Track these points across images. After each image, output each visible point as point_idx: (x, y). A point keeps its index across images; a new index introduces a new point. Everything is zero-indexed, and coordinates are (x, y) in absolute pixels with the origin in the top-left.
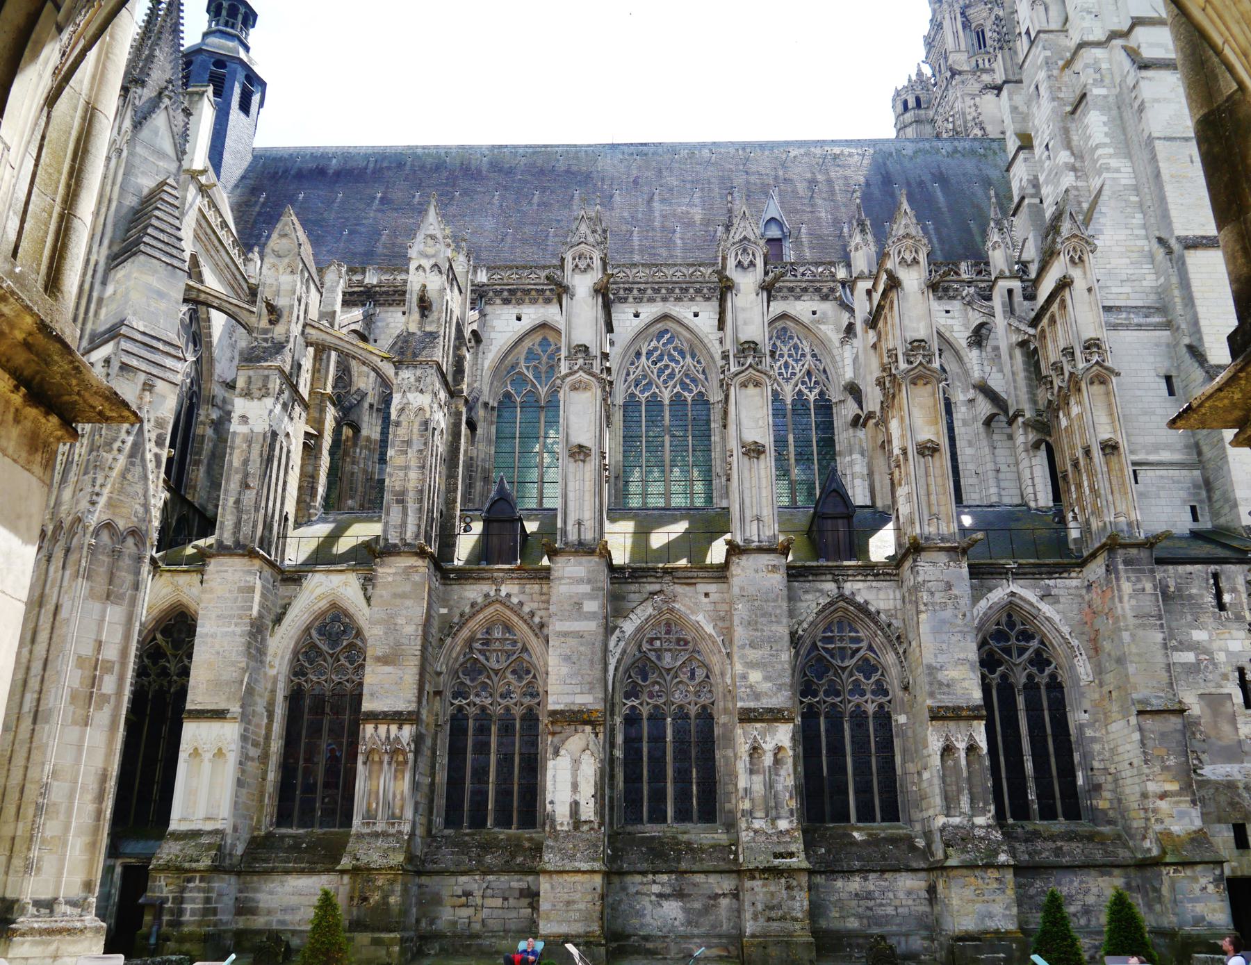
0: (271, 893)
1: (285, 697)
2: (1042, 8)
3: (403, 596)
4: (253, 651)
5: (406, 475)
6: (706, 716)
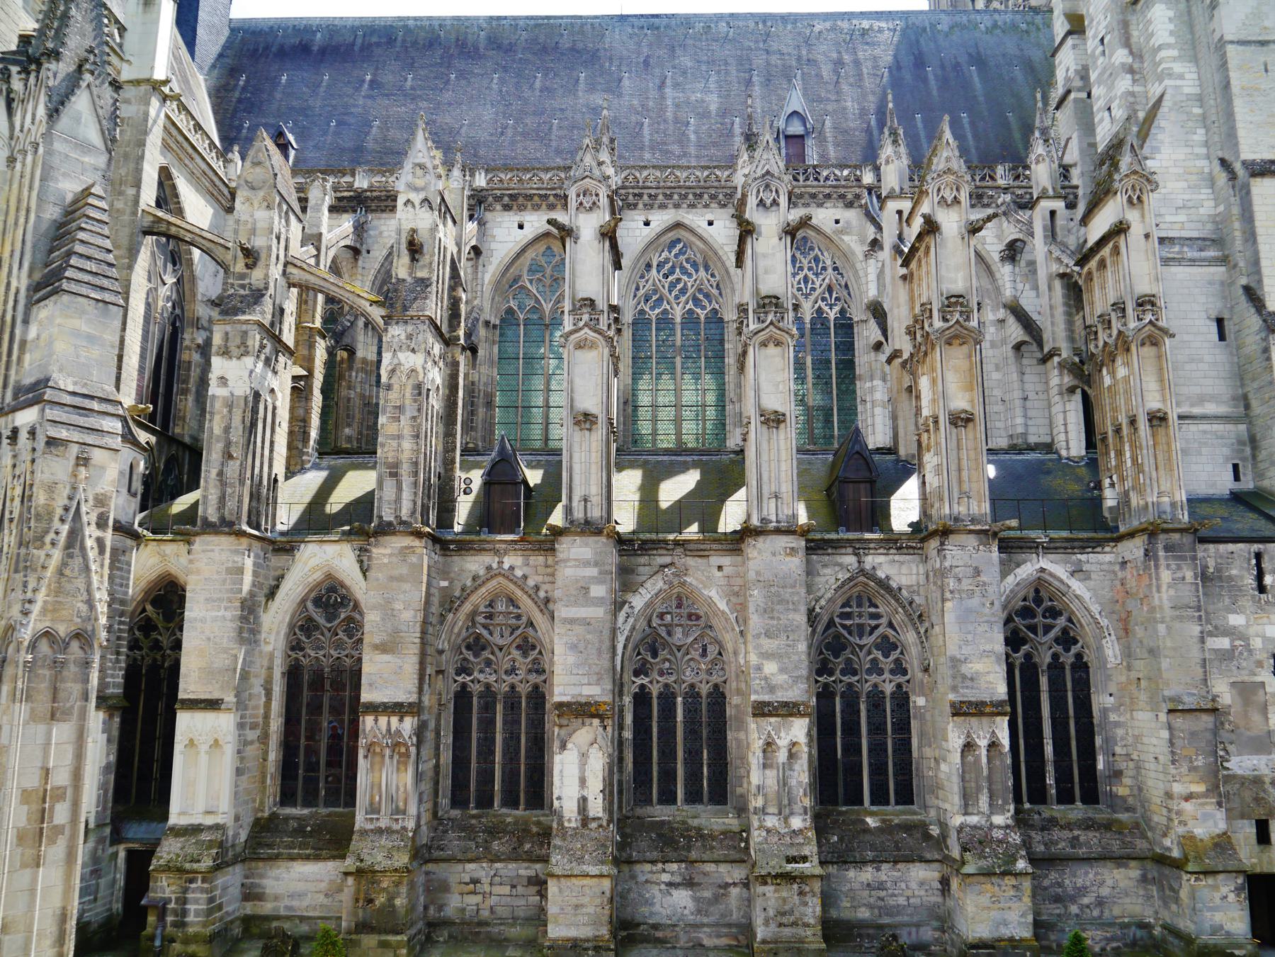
0: (277, 879)
1: (283, 673)
3: (400, 579)
4: (245, 635)
5: (399, 445)
6: (718, 697)
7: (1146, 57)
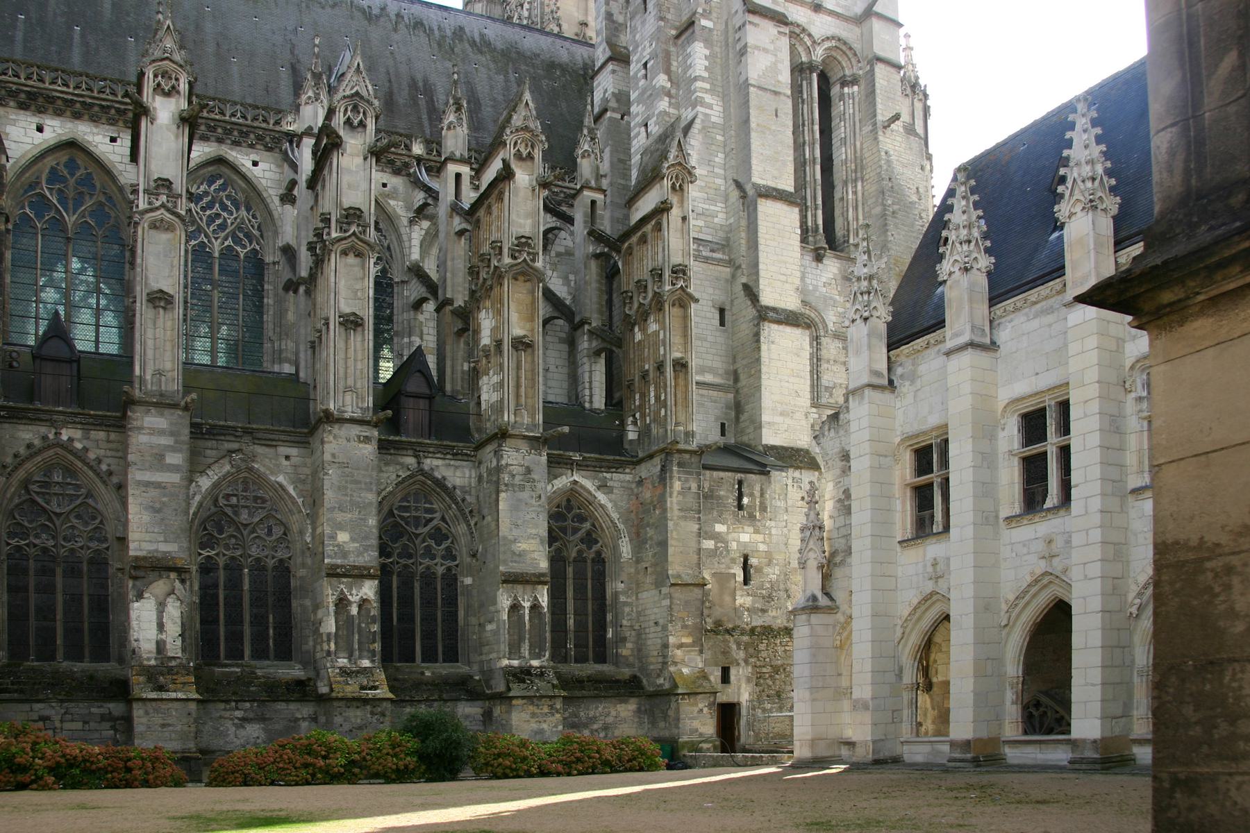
6: (283, 569)
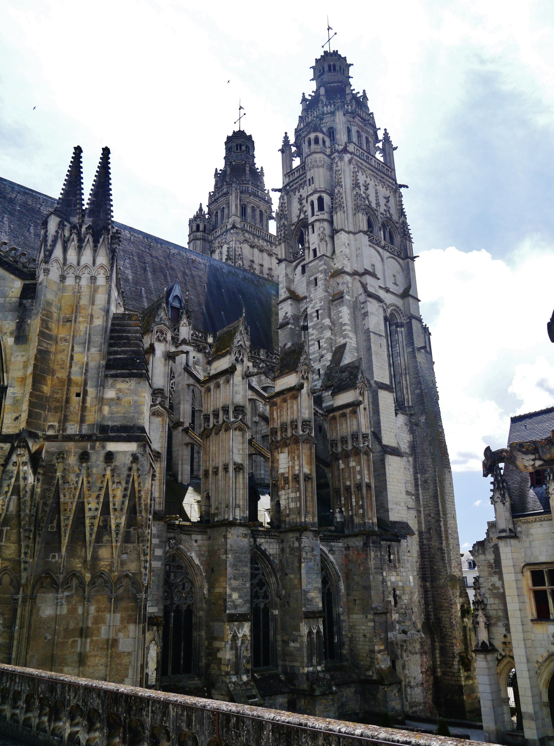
2: (325, 243)
6: (190, 612)
7: (337, 325)
